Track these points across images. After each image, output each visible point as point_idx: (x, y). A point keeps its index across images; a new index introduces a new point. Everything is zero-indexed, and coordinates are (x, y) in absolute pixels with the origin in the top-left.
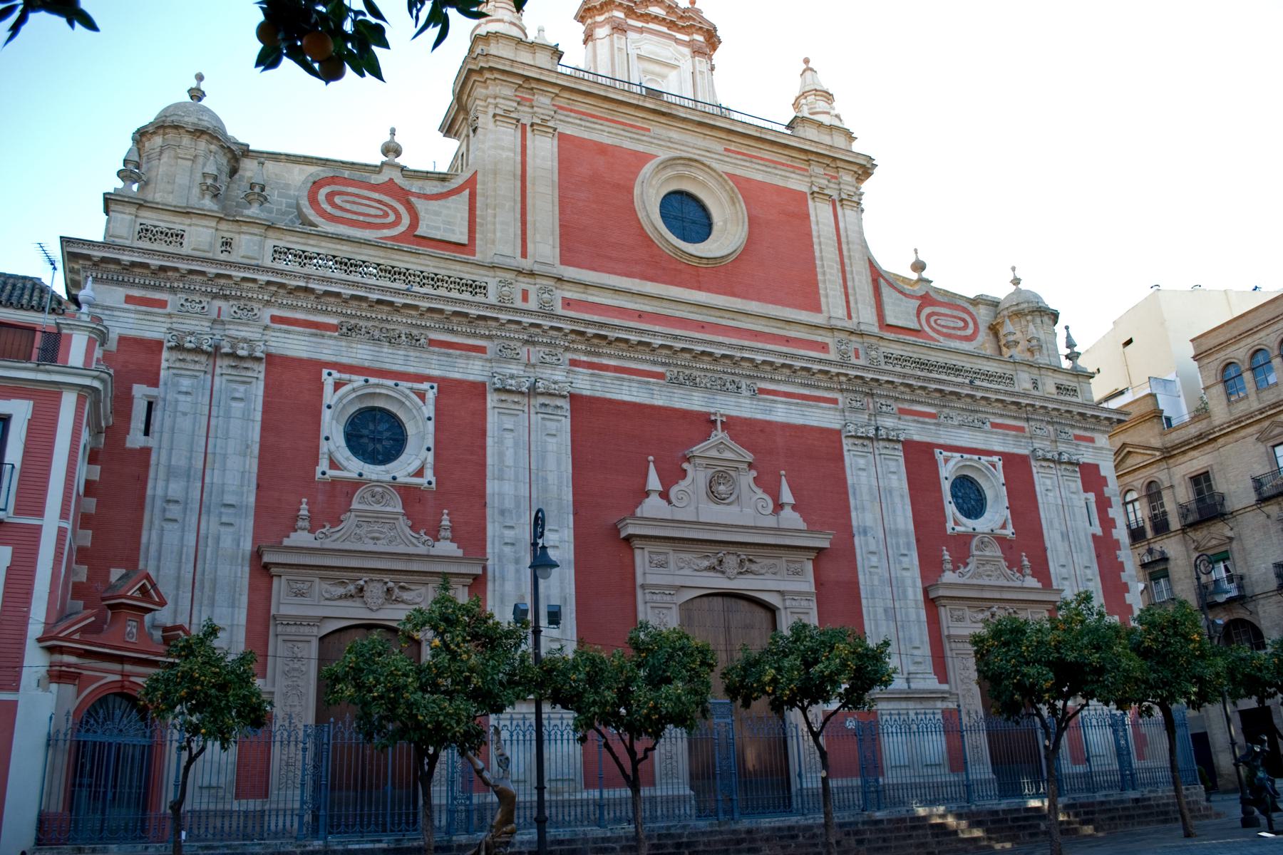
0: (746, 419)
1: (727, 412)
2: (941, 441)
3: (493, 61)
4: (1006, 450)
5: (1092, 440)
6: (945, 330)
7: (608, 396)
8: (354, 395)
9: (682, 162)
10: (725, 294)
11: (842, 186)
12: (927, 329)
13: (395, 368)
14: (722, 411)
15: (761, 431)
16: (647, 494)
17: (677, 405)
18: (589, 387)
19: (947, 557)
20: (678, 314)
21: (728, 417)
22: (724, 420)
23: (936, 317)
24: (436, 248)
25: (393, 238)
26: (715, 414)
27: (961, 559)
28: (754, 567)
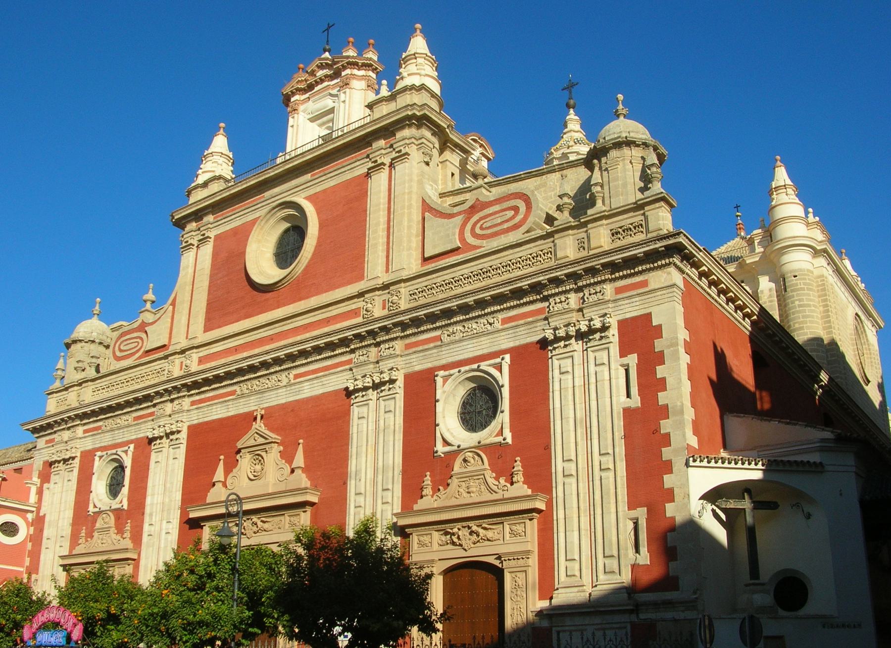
0: (283, 404)
1: (266, 405)
2: (444, 362)
3: (176, 215)
4: (517, 343)
5: (645, 284)
6: (506, 226)
7: (206, 419)
8: (105, 463)
9: (277, 209)
10: (294, 302)
11: (394, 147)
12: (470, 240)
13: (120, 441)
14: (262, 406)
15: (292, 411)
16: (214, 485)
17: (242, 411)
18: (196, 418)
19: (428, 480)
20: (258, 336)
21: (266, 409)
22: (263, 412)
23: (481, 222)
24: (155, 354)
25: (140, 358)
26: (257, 410)
27: (442, 481)
28: (266, 526)
